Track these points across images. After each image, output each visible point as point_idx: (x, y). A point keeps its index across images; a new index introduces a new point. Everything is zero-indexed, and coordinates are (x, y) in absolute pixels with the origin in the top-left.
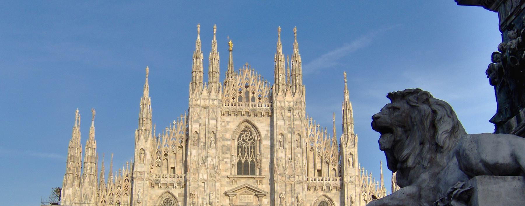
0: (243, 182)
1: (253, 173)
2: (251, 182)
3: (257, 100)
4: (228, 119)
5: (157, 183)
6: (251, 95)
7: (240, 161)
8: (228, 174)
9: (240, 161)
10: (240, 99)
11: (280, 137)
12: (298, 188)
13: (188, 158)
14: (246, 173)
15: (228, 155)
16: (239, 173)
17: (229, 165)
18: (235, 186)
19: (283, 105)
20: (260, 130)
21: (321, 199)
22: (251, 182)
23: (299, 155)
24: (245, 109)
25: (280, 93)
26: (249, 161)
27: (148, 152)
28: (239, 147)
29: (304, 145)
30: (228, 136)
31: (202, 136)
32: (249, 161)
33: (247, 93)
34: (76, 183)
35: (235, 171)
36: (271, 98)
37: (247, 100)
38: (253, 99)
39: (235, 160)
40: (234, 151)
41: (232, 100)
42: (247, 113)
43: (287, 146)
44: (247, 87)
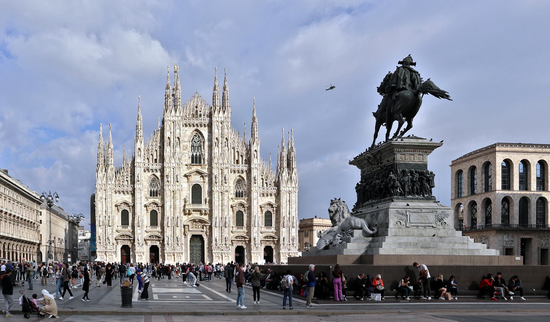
0: (194, 168)
1: (200, 162)
2: (199, 168)
3: (203, 116)
6: (199, 113)
7: (193, 155)
8: (186, 163)
9: (193, 155)
12: (226, 171)
15: (186, 152)
16: (193, 162)
17: (187, 158)
18: (190, 170)
19: (217, 119)
20: (204, 135)
22: (199, 168)
23: (226, 151)
25: (216, 112)
26: (198, 154)
29: (229, 145)
32: (198, 154)
33: (197, 111)
34: (104, 170)
38: (200, 115)
39: (191, 154)
40: (189, 149)
42: (197, 124)
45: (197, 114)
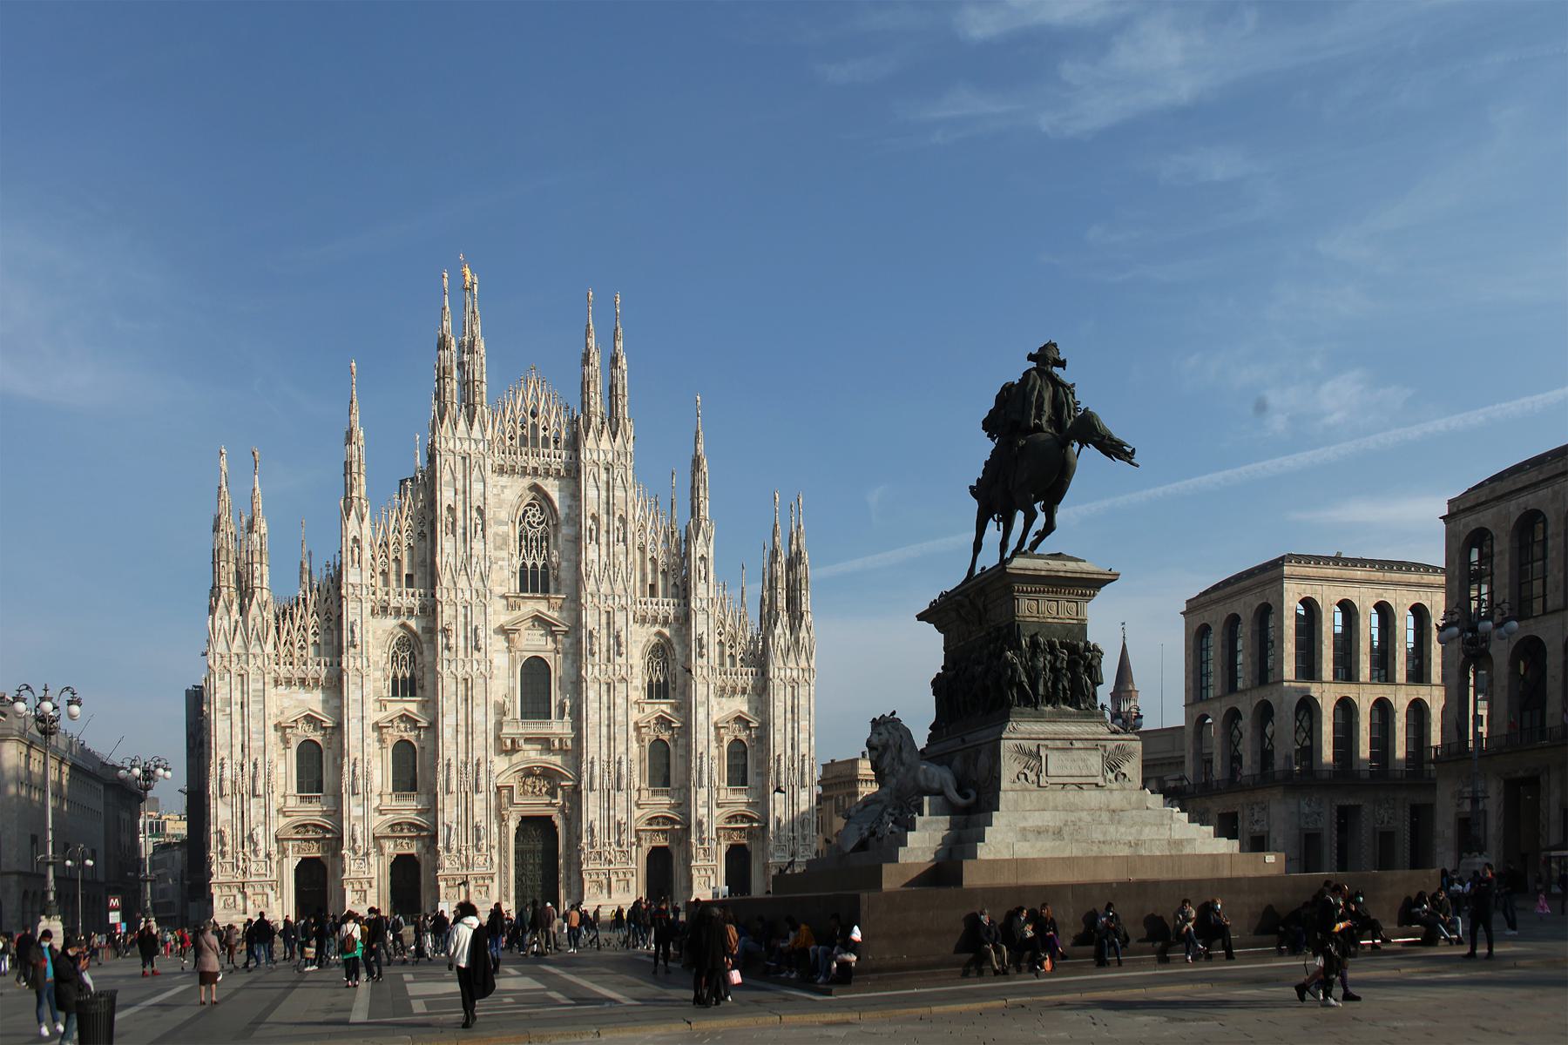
0: (531, 606)
2: (542, 607)
4: (505, 480)
5: (385, 610)
6: (541, 433)
8: (504, 590)
10: (524, 439)
11: (589, 522)
12: (620, 619)
13: (438, 559)
14: (534, 590)
15: (504, 554)
16: (523, 589)
17: (506, 573)
21: (654, 640)
23: (622, 558)
24: (533, 463)
26: (540, 564)
27: (365, 545)
28: (523, 537)
29: (630, 537)
30: (503, 515)
31: (459, 514)
32: (540, 564)
33: (535, 427)
35: (514, 585)
36: (574, 444)
37: (535, 445)
40: (513, 545)
41: (508, 442)
42: (535, 469)
43: (603, 540)
44: (534, 415)
45: (535, 437)
